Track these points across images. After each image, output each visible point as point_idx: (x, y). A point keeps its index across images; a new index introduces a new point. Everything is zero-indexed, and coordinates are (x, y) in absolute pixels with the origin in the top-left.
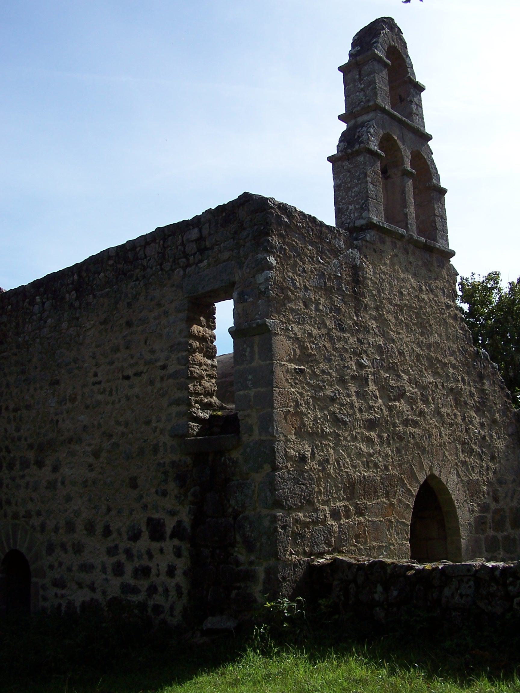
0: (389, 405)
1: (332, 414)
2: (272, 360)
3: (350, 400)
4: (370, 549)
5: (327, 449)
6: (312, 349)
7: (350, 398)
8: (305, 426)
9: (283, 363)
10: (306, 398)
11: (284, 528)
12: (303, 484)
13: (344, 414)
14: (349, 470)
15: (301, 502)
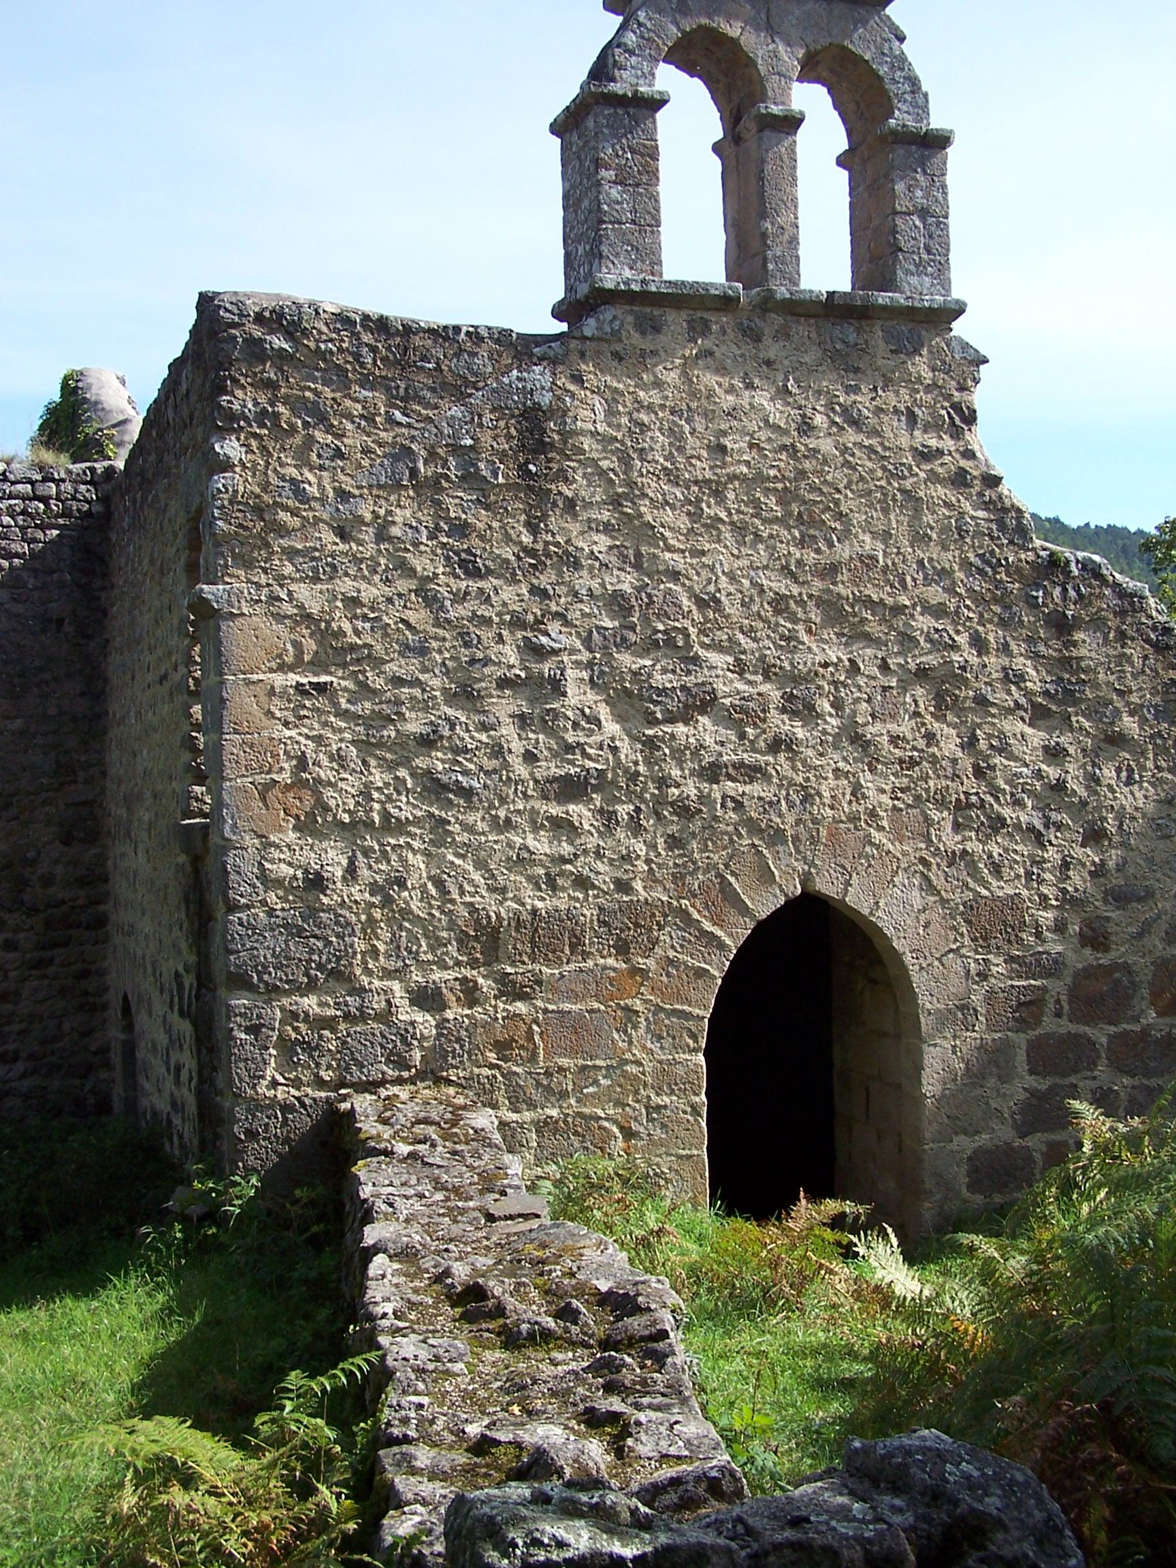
0: (644, 735)
1: (423, 775)
2: (221, 674)
3: (489, 737)
4: (548, 1074)
5: (400, 856)
6: (357, 633)
7: (492, 733)
8: (327, 809)
9: (255, 677)
10: (335, 747)
11: (254, 1030)
12: (315, 937)
13: (465, 773)
14: (478, 899)
15: (307, 974)
